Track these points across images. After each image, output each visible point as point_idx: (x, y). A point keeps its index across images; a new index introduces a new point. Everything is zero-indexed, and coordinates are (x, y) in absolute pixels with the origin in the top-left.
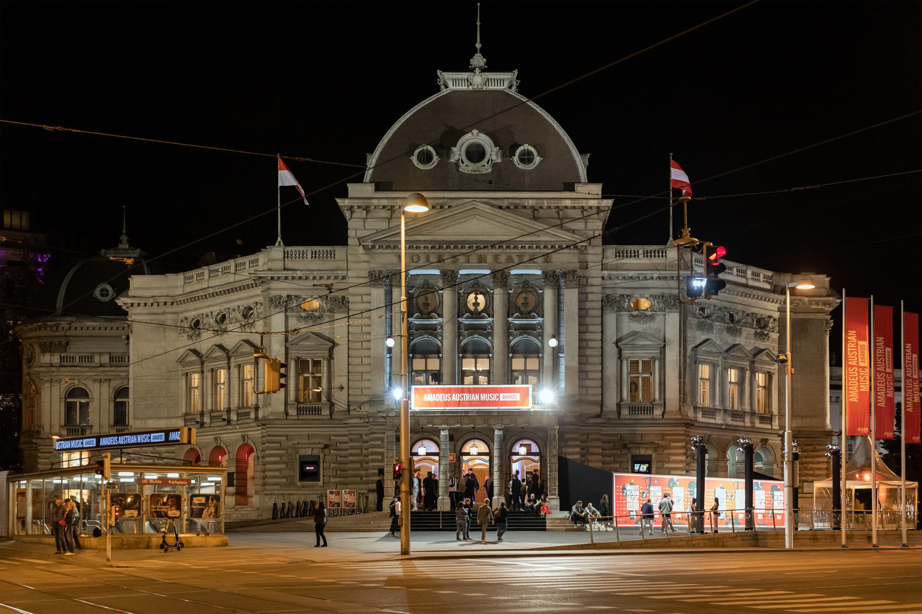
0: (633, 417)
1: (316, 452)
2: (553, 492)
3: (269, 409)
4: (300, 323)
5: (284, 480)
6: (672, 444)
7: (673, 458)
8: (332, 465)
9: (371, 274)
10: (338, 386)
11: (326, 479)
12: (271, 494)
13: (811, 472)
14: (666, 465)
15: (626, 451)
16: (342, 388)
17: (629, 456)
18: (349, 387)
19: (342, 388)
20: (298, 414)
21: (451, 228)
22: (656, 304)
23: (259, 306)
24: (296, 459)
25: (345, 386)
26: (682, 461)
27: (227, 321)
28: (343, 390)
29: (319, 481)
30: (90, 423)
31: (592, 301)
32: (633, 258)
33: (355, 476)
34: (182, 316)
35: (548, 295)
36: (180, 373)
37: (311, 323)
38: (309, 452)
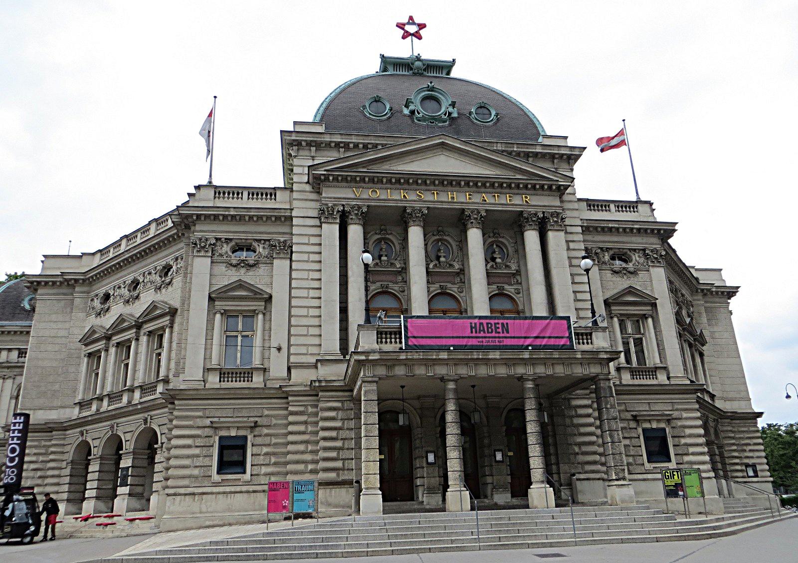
1: (242, 433)
4: (229, 271)
5: (196, 472)
6: (685, 415)
7: (688, 431)
8: (265, 450)
9: (322, 211)
11: (256, 470)
12: (175, 495)
13: (751, 454)
14: (683, 441)
15: (633, 424)
16: (279, 349)
17: (640, 430)
19: (279, 349)
20: (220, 381)
21: (415, 163)
22: (638, 259)
23: (179, 260)
24: (215, 442)
25: (285, 347)
26: (699, 436)
27: (140, 287)
28: (281, 352)
31: (574, 250)
32: (605, 213)
33: (297, 462)
34: (93, 294)
35: (531, 238)
36: (83, 355)
37: (243, 271)
38: (233, 433)
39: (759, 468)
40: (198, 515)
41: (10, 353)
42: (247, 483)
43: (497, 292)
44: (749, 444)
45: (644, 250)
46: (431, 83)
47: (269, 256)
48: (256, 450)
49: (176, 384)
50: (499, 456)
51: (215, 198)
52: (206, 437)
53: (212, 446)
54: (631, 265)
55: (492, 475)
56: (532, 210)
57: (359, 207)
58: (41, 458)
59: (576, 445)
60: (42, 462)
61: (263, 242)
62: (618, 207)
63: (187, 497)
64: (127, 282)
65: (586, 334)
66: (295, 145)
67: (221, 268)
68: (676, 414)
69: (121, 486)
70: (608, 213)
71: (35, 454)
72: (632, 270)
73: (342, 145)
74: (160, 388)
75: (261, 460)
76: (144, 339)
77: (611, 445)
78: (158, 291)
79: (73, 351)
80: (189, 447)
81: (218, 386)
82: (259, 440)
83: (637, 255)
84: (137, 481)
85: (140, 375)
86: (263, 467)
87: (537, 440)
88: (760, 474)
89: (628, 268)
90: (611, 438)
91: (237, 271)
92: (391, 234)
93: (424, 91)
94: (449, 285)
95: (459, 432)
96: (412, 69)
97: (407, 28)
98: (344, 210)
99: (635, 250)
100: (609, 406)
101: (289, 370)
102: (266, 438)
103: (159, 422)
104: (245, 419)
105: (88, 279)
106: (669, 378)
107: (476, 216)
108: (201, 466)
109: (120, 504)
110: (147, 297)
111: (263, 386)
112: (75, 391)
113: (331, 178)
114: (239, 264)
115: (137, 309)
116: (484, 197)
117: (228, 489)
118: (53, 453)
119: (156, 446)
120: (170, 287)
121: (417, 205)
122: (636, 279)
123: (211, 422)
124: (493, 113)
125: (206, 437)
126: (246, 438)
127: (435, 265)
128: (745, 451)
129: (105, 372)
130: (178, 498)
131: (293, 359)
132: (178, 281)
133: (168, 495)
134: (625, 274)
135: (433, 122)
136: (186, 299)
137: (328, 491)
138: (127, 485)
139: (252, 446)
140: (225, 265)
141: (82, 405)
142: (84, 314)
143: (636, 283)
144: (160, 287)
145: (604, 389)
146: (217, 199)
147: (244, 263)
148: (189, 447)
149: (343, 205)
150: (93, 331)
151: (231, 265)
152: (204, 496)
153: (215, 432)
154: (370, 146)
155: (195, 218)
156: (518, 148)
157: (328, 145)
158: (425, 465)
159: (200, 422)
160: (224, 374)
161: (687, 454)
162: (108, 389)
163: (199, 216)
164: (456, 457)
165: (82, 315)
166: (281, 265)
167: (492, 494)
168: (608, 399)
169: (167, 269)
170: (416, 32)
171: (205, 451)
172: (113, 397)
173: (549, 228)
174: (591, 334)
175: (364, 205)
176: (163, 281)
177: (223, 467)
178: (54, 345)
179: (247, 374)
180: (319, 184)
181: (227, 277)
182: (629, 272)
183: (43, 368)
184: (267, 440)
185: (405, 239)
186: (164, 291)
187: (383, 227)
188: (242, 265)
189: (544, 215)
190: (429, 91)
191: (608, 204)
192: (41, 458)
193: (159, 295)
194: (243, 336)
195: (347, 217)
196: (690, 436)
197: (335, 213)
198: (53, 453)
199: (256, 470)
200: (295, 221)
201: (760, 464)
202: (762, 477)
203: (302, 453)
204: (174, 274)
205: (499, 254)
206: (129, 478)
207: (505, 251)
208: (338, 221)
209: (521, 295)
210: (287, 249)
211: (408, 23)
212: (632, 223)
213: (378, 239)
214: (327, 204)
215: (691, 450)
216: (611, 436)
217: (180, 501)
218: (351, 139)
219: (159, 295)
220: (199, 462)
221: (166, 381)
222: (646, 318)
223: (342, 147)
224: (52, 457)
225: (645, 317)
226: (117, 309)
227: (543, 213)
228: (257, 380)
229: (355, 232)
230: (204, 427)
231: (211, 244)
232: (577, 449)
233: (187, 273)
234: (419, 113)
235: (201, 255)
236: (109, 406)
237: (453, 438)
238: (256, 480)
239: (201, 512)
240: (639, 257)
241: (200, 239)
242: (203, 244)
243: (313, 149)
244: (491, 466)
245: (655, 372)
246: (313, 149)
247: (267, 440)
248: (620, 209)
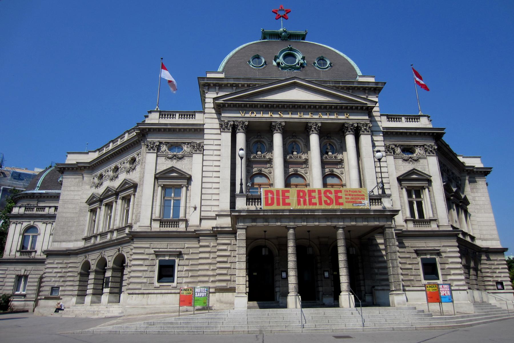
0: (417, 229)
2: (398, 288)
3: (138, 224)
8: (186, 268)
10: (193, 206)
11: (180, 280)
12: (133, 294)
13: (499, 275)
14: (447, 266)
15: (415, 255)
16: (195, 208)
18: (201, 206)
19: (195, 208)
20: (160, 227)
22: (419, 151)
24: (156, 263)
29: (173, 282)
30: (36, 249)
32: (398, 122)
37: (175, 161)
38: (167, 258)
39: (504, 283)
40: (146, 306)
41: (50, 209)
42: (175, 288)
43: (329, 173)
44: (498, 268)
45: (423, 146)
46: (290, 46)
47: (190, 152)
48: (180, 268)
49: (136, 228)
50: (326, 274)
51: (160, 118)
52: (151, 260)
53: (155, 265)
54: (415, 155)
55: (322, 286)
56: (351, 122)
57: (243, 123)
58: (64, 270)
59: (376, 268)
60: (64, 272)
61: (187, 144)
62: (407, 119)
63: (140, 295)
64: (112, 168)
65: (378, 200)
66: (207, 86)
67: (161, 160)
68: (442, 249)
69: (105, 288)
70: (400, 122)
71: (61, 268)
72: (416, 158)
73: (234, 85)
74: (127, 231)
75: (183, 274)
76: (119, 201)
77: (392, 269)
78: (128, 173)
79: (82, 208)
80: (141, 265)
81: (158, 230)
82: (182, 262)
83: (418, 149)
84: (115, 285)
85: (117, 222)
86: (184, 278)
87: (345, 265)
88: (505, 287)
89: (413, 157)
90: (391, 264)
91: (172, 161)
92: (264, 138)
93: (286, 51)
94: (299, 169)
95: (295, 259)
96: (280, 37)
97: (279, 13)
98: (234, 124)
99: (417, 146)
100: (391, 244)
101: (201, 219)
102: (186, 261)
103: (126, 251)
104: (174, 250)
105: (91, 166)
106: (438, 226)
107: (315, 127)
108: (148, 277)
109: (105, 298)
110: (122, 176)
111: (185, 230)
112: (83, 231)
113: (227, 105)
114: (173, 157)
115: (116, 184)
116: (320, 115)
117: (163, 291)
118: (70, 267)
119: (124, 265)
120: (134, 171)
121: (279, 121)
122: (418, 164)
123: (154, 251)
124: (328, 63)
125: (151, 260)
126: (174, 261)
127: (291, 158)
128: (496, 272)
129: (99, 220)
130: (134, 296)
131: (203, 214)
132: (138, 168)
133: (129, 294)
134: (411, 161)
135: (291, 70)
136: (142, 178)
137: (221, 294)
138: (109, 287)
139: (179, 265)
140: (164, 157)
141: (86, 239)
142: (89, 186)
143: (419, 166)
144: (129, 171)
145: (388, 233)
146: (161, 118)
147: (176, 157)
148: (141, 265)
149: (234, 121)
150: (93, 196)
151: (168, 158)
152: (150, 295)
153: (157, 257)
154: (251, 85)
155: (147, 130)
156: (342, 84)
157: (226, 85)
158: (280, 279)
159: (147, 251)
160: (162, 222)
161: (450, 275)
162: (100, 230)
163: (150, 129)
164: (293, 275)
165: (88, 187)
166: (197, 158)
167: (322, 298)
168: (391, 240)
169: (133, 160)
170: (284, 15)
171: (150, 268)
172: (103, 235)
173: (361, 133)
174: (380, 199)
175: (247, 121)
176: (131, 168)
177: (160, 278)
178: (72, 205)
179: (175, 222)
180: (220, 109)
181: (165, 164)
182: (413, 160)
183: (66, 218)
184: (187, 262)
185: (272, 141)
186: (131, 173)
187: (259, 134)
188: (175, 157)
189: (358, 125)
190: (289, 50)
191: (400, 117)
192: (64, 270)
193: (128, 175)
194: (174, 200)
195: (237, 128)
196: (452, 263)
197: (229, 126)
198: (70, 267)
199: (180, 280)
200: (206, 131)
201: (505, 281)
202: (507, 289)
203: (207, 270)
204: (137, 163)
205: (330, 149)
206: (110, 283)
207: (335, 147)
208: (230, 131)
209: (344, 175)
210: (200, 148)
211: (280, 10)
212: (416, 129)
213: (256, 141)
214: (224, 121)
215: (453, 272)
216: (392, 263)
217: (136, 298)
218: (240, 81)
219: (128, 175)
220: (148, 274)
221: (131, 227)
222: (425, 189)
223: (234, 86)
224: (70, 270)
225: (423, 188)
226: (107, 184)
227: (358, 123)
228: (182, 227)
229: (241, 138)
230: (150, 254)
231: (156, 146)
232: (376, 271)
233: (143, 162)
234: (282, 64)
235: (151, 152)
236: (100, 240)
237: (292, 263)
238: (179, 286)
239: (147, 305)
240: (420, 149)
241: (150, 143)
242: (152, 146)
243: (217, 88)
244: (322, 280)
245: (430, 222)
246: (217, 88)
247: (187, 262)
248: (408, 120)
